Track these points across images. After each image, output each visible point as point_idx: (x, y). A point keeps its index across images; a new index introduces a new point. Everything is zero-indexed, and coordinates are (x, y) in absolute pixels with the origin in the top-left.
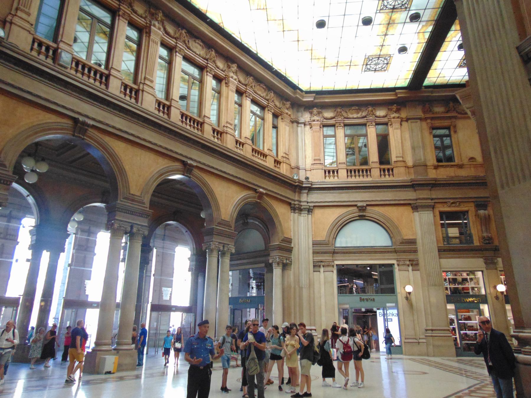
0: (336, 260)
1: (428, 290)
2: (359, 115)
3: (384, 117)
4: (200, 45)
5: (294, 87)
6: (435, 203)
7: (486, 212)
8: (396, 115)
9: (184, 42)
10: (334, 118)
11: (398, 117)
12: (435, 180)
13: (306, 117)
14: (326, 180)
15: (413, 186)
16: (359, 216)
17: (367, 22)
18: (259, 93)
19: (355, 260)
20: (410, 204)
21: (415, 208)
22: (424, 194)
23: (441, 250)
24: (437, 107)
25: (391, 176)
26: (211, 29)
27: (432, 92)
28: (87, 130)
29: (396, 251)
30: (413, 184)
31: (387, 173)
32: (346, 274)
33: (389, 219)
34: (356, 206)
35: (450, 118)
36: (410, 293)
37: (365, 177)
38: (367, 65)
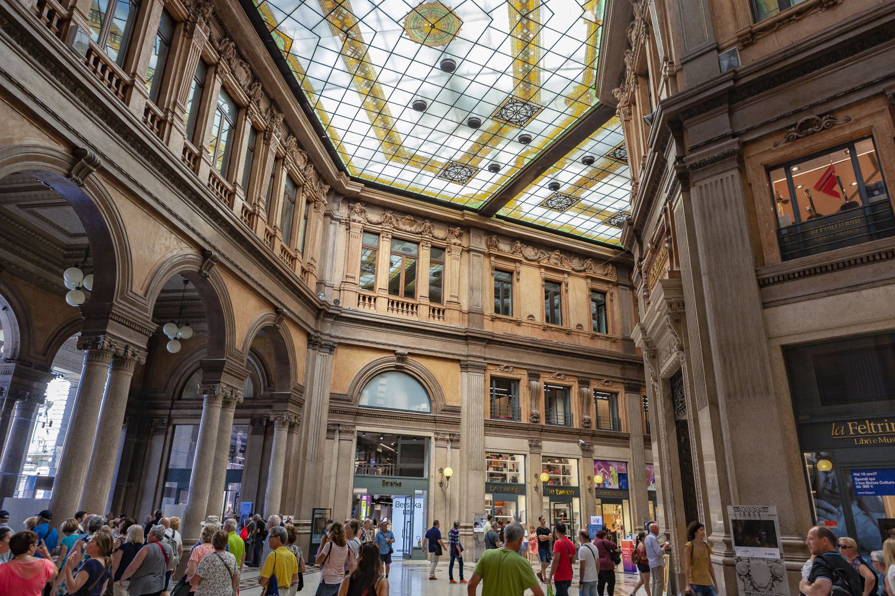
0: (359, 425)
1: (468, 475)
2: (413, 229)
5: (341, 168)
7: (538, 384)
8: (458, 242)
9: (229, 60)
10: (380, 224)
11: (460, 245)
12: (492, 335)
13: (342, 212)
15: (466, 338)
16: (396, 367)
17: (474, 124)
18: (298, 163)
19: (383, 427)
20: (459, 361)
21: (465, 366)
22: (477, 350)
23: (488, 426)
24: (503, 243)
25: (441, 319)
26: (268, 54)
28: (90, 171)
29: (435, 421)
30: (467, 336)
31: (436, 314)
32: (365, 445)
33: (432, 378)
34: (393, 352)
35: (515, 261)
36: (448, 478)
37: (410, 314)
38: (446, 170)
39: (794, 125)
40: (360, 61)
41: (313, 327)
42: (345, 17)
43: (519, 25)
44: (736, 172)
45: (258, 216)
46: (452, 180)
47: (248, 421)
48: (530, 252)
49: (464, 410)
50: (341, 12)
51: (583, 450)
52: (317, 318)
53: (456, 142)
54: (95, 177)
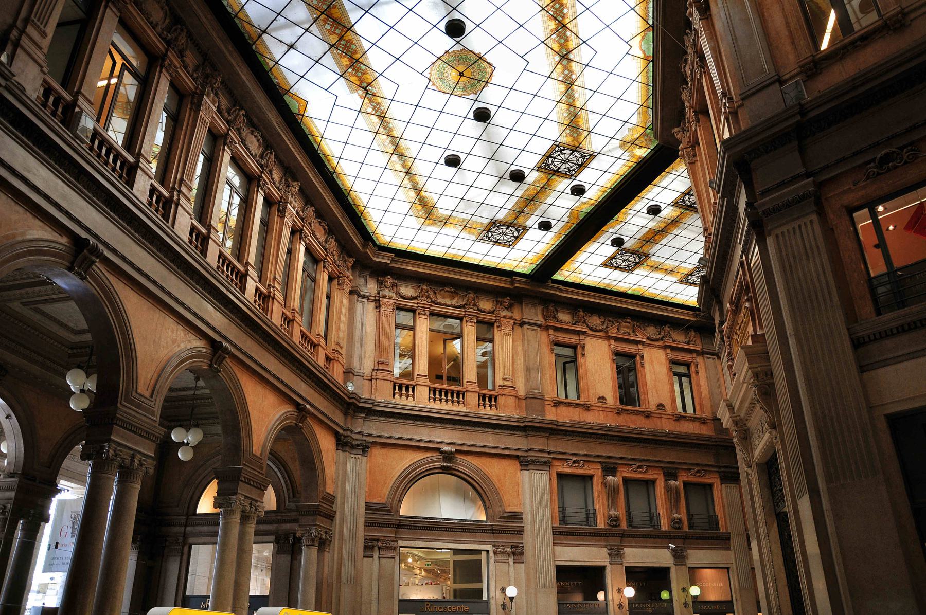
0: (401, 539)
1: (536, 594)
2: (454, 302)
3: (489, 312)
4: (258, 141)
6: (553, 458)
7: (616, 479)
8: (509, 314)
10: (415, 298)
11: (511, 318)
12: (556, 423)
13: (371, 287)
14: (394, 401)
15: (525, 429)
16: (442, 468)
18: (318, 235)
19: (430, 540)
20: (517, 457)
21: (525, 463)
22: (538, 443)
23: (556, 533)
24: (563, 312)
26: (280, 119)
27: (560, 290)
28: (93, 262)
29: (492, 531)
30: (526, 426)
33: (485, 477)
34: (438, 450)
36: (512, 599)
39: (873, 160)
40: (382, 118)
41: (342, 424)
42: (364, 73)
43: (559, 66)
44: (814, 217)
45: (273, 298)
46: (497, 242)
47: (272, 538)
48: (596, 321)
49: (527, 518)
50: (359, 68)
51: (674, 556)
52: (346, 414)
53: (497, 200)
54: (99, 268)
